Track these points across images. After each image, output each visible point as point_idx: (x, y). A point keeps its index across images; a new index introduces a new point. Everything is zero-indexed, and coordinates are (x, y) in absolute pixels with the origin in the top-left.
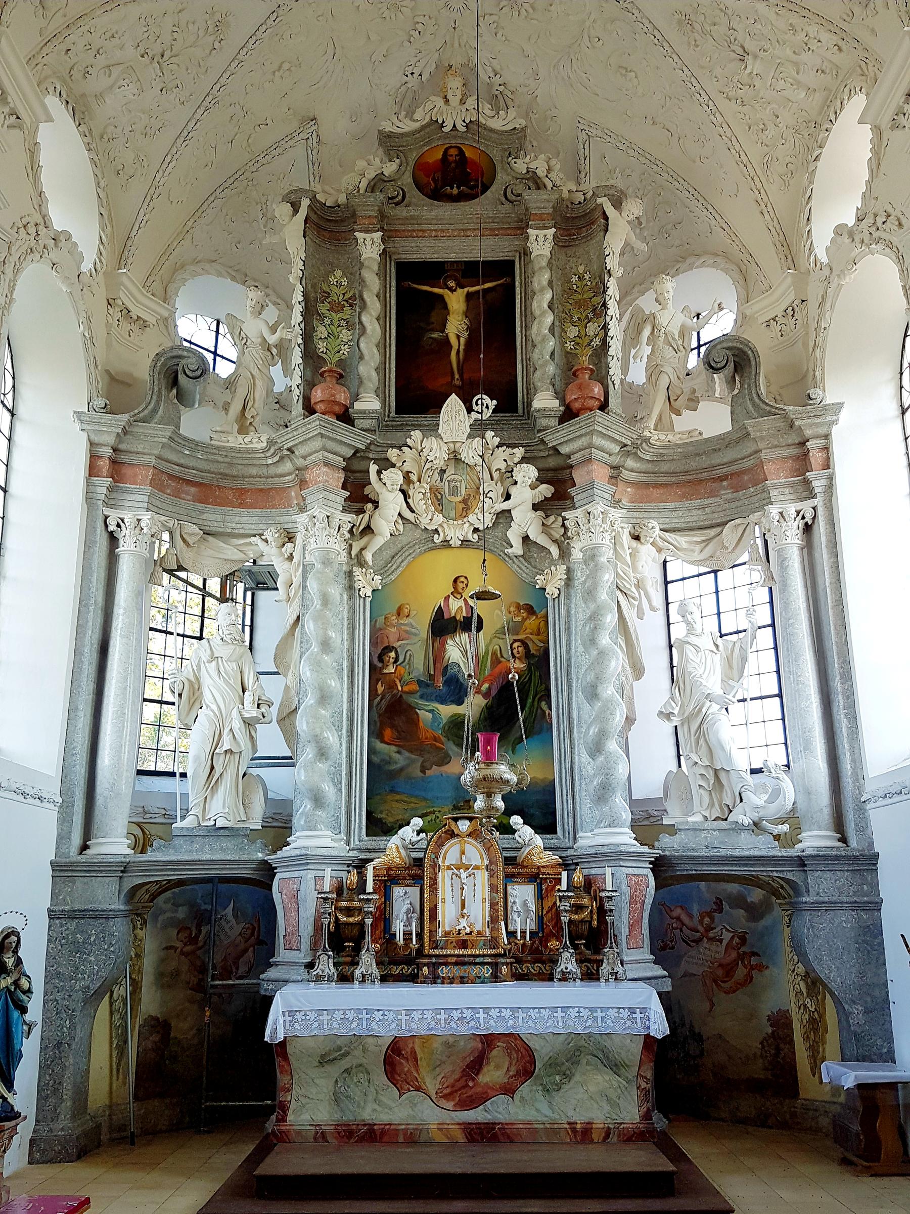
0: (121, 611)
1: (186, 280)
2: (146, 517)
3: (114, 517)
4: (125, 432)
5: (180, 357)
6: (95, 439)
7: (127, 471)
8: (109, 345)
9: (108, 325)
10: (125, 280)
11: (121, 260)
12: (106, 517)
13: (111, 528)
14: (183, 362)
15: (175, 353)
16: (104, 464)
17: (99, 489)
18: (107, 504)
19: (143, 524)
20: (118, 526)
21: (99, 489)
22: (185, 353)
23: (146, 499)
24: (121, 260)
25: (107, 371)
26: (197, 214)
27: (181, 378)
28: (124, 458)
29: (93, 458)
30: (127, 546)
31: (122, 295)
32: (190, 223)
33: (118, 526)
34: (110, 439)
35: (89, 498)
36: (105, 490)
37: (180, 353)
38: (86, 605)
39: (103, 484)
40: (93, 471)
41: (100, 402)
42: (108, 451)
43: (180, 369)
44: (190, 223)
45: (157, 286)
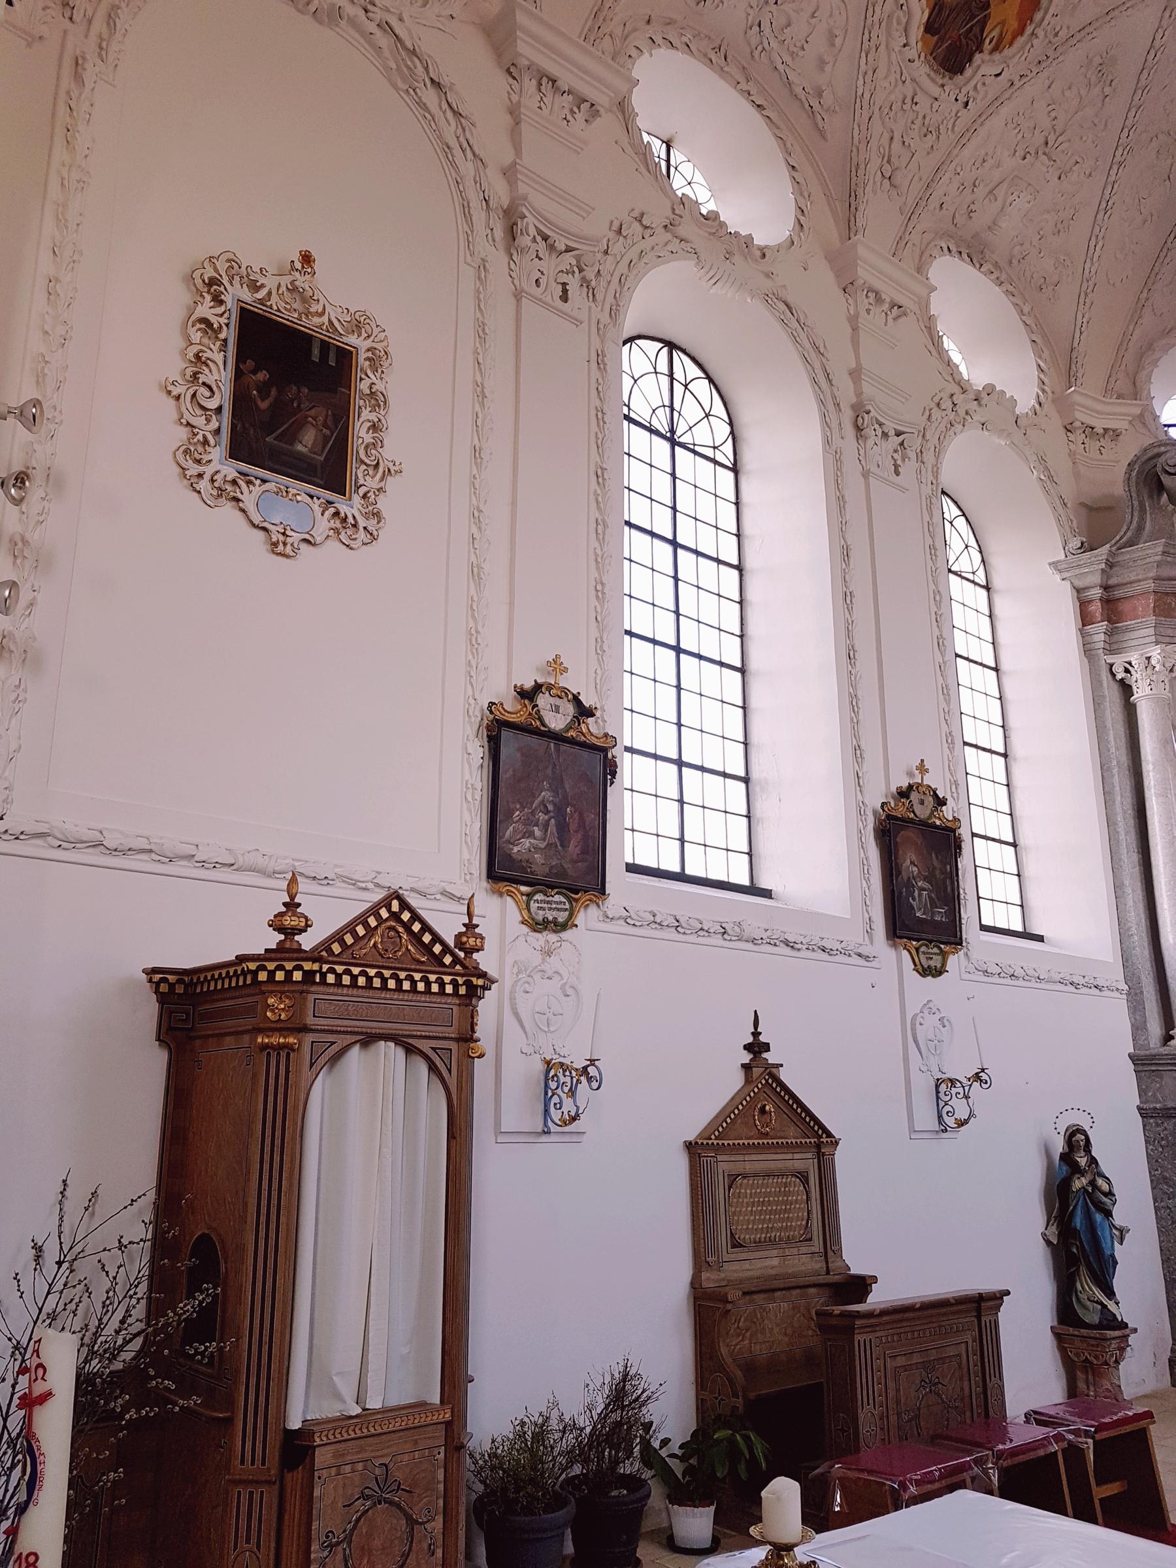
0: (1151, 767)
1: (1158, 360)
2: (1156, 653)
3: (1119, 662)
4: (1110, 565)
5: (1159, 455)
6: (1080, 584)
7: (1125, 607)
8: (1077, 475)
9: (1072, 454)
10: (1078, 398)
11: (1071, 377)
12: (1111, 665)
13: (1119, 677)
14: (1162, 460)
15: (1150, 454)
16: (1096, 608)
17: (1096, 638)
18: (1111, 652)
19: (1153, 662)
20: (1127, 671)
21: (1096, 638)
22: (1163, 449)
23: (1151, 631)
24: (1071, 377)
25: (1083, 504)
26: (1148, 285)
27: (1165, 479)
28: (1118, 593)
29: (1083, 606)
30: (1141, 692)
31: (1078, 415)
32: (1145, 295)
33: (1127, 671)
34: (1096, 579)
35: (1088, 650)
36: (1102, 637)
37: (1156, 450)
38: (1109, 769)
39: (1099, 631)
40: (1085, 619)
41: (1075, 543)
42: (1096, 593)
43: (1159, 469)
44: (1145, 295)
45: (1122, 384)
